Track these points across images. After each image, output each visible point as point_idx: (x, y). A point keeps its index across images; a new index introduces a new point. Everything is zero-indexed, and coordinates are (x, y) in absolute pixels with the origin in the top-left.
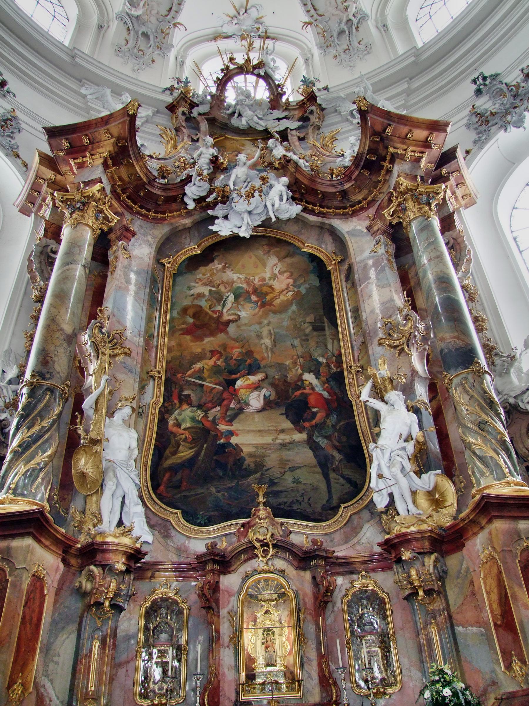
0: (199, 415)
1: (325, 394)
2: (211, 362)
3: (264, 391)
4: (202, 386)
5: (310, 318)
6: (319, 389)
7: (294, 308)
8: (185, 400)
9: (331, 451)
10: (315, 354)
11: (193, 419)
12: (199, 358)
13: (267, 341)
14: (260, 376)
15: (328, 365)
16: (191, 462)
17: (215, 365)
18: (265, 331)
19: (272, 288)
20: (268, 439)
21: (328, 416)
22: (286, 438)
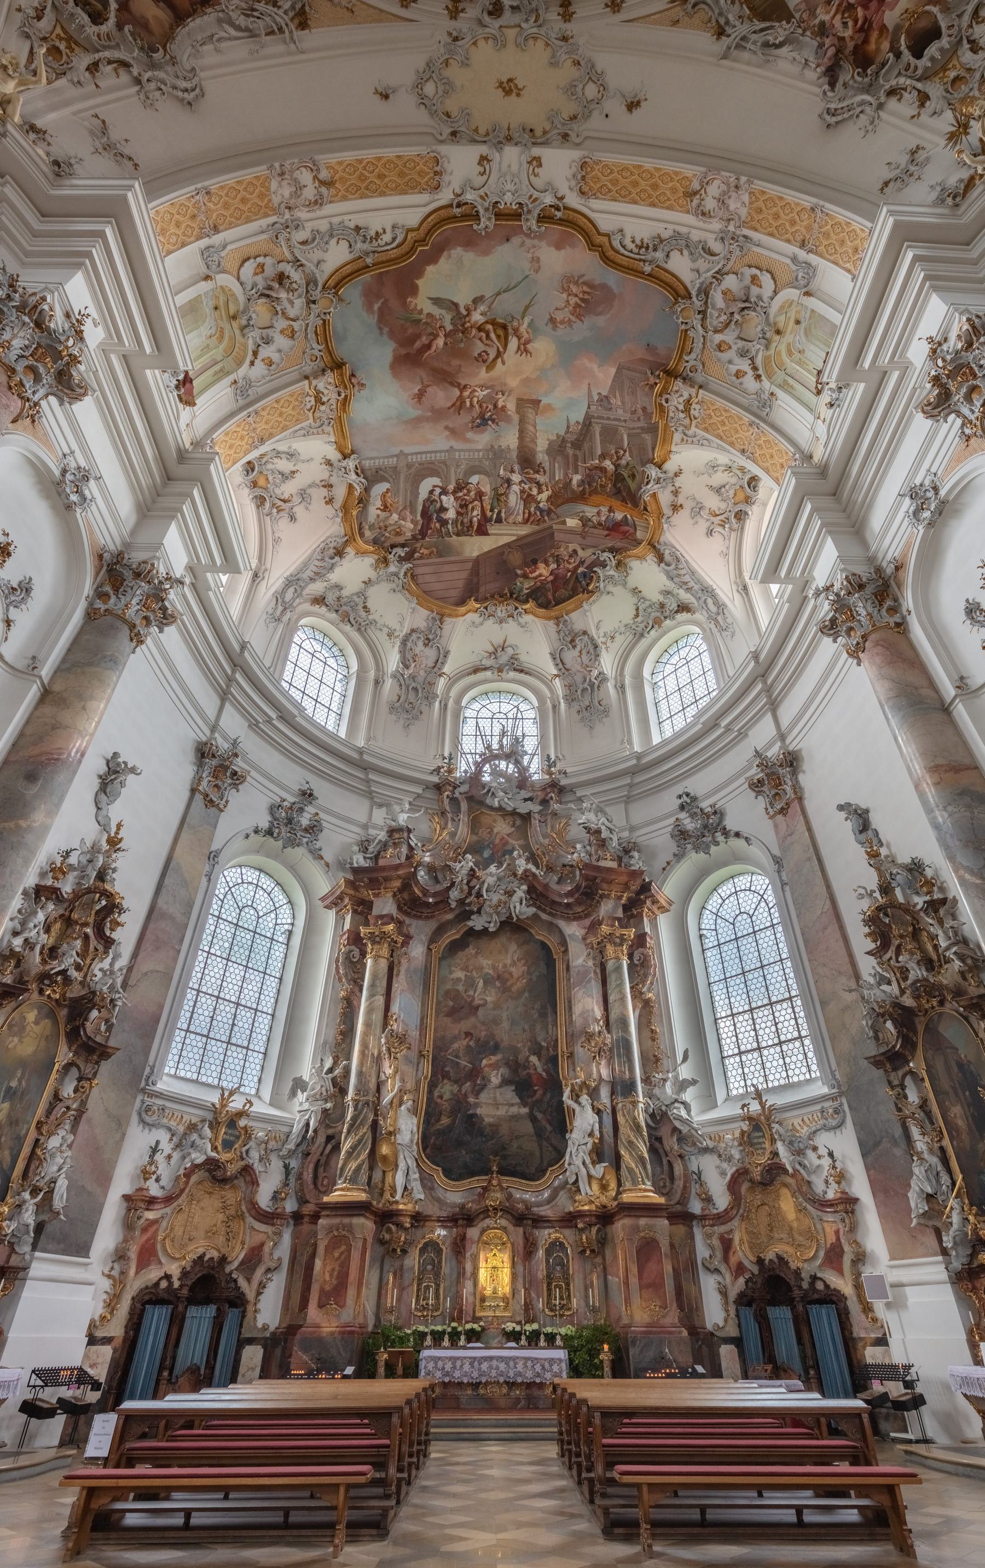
0: (455, 1088)
1: (544, 1074)
2: (465, 1042)
3: (501, 1070)
4: (458, 1063)
5: (537, 1006)
6: (540, 1070)
7: (526, 994)
8: (446, 1076)
9: (544, 1123)
10: (539, 1039)
11: (452, 1092)
12: (456, 1038)
13: (505, 1025)
14: (499, 1056)
15: (548, 1049)
16: (450, 1128)
17: (468, 1046)
18: (504, 1015)
19: (511, 974)
20: (502, 1112)
21: (544, 1094)
22: (514, 1110)
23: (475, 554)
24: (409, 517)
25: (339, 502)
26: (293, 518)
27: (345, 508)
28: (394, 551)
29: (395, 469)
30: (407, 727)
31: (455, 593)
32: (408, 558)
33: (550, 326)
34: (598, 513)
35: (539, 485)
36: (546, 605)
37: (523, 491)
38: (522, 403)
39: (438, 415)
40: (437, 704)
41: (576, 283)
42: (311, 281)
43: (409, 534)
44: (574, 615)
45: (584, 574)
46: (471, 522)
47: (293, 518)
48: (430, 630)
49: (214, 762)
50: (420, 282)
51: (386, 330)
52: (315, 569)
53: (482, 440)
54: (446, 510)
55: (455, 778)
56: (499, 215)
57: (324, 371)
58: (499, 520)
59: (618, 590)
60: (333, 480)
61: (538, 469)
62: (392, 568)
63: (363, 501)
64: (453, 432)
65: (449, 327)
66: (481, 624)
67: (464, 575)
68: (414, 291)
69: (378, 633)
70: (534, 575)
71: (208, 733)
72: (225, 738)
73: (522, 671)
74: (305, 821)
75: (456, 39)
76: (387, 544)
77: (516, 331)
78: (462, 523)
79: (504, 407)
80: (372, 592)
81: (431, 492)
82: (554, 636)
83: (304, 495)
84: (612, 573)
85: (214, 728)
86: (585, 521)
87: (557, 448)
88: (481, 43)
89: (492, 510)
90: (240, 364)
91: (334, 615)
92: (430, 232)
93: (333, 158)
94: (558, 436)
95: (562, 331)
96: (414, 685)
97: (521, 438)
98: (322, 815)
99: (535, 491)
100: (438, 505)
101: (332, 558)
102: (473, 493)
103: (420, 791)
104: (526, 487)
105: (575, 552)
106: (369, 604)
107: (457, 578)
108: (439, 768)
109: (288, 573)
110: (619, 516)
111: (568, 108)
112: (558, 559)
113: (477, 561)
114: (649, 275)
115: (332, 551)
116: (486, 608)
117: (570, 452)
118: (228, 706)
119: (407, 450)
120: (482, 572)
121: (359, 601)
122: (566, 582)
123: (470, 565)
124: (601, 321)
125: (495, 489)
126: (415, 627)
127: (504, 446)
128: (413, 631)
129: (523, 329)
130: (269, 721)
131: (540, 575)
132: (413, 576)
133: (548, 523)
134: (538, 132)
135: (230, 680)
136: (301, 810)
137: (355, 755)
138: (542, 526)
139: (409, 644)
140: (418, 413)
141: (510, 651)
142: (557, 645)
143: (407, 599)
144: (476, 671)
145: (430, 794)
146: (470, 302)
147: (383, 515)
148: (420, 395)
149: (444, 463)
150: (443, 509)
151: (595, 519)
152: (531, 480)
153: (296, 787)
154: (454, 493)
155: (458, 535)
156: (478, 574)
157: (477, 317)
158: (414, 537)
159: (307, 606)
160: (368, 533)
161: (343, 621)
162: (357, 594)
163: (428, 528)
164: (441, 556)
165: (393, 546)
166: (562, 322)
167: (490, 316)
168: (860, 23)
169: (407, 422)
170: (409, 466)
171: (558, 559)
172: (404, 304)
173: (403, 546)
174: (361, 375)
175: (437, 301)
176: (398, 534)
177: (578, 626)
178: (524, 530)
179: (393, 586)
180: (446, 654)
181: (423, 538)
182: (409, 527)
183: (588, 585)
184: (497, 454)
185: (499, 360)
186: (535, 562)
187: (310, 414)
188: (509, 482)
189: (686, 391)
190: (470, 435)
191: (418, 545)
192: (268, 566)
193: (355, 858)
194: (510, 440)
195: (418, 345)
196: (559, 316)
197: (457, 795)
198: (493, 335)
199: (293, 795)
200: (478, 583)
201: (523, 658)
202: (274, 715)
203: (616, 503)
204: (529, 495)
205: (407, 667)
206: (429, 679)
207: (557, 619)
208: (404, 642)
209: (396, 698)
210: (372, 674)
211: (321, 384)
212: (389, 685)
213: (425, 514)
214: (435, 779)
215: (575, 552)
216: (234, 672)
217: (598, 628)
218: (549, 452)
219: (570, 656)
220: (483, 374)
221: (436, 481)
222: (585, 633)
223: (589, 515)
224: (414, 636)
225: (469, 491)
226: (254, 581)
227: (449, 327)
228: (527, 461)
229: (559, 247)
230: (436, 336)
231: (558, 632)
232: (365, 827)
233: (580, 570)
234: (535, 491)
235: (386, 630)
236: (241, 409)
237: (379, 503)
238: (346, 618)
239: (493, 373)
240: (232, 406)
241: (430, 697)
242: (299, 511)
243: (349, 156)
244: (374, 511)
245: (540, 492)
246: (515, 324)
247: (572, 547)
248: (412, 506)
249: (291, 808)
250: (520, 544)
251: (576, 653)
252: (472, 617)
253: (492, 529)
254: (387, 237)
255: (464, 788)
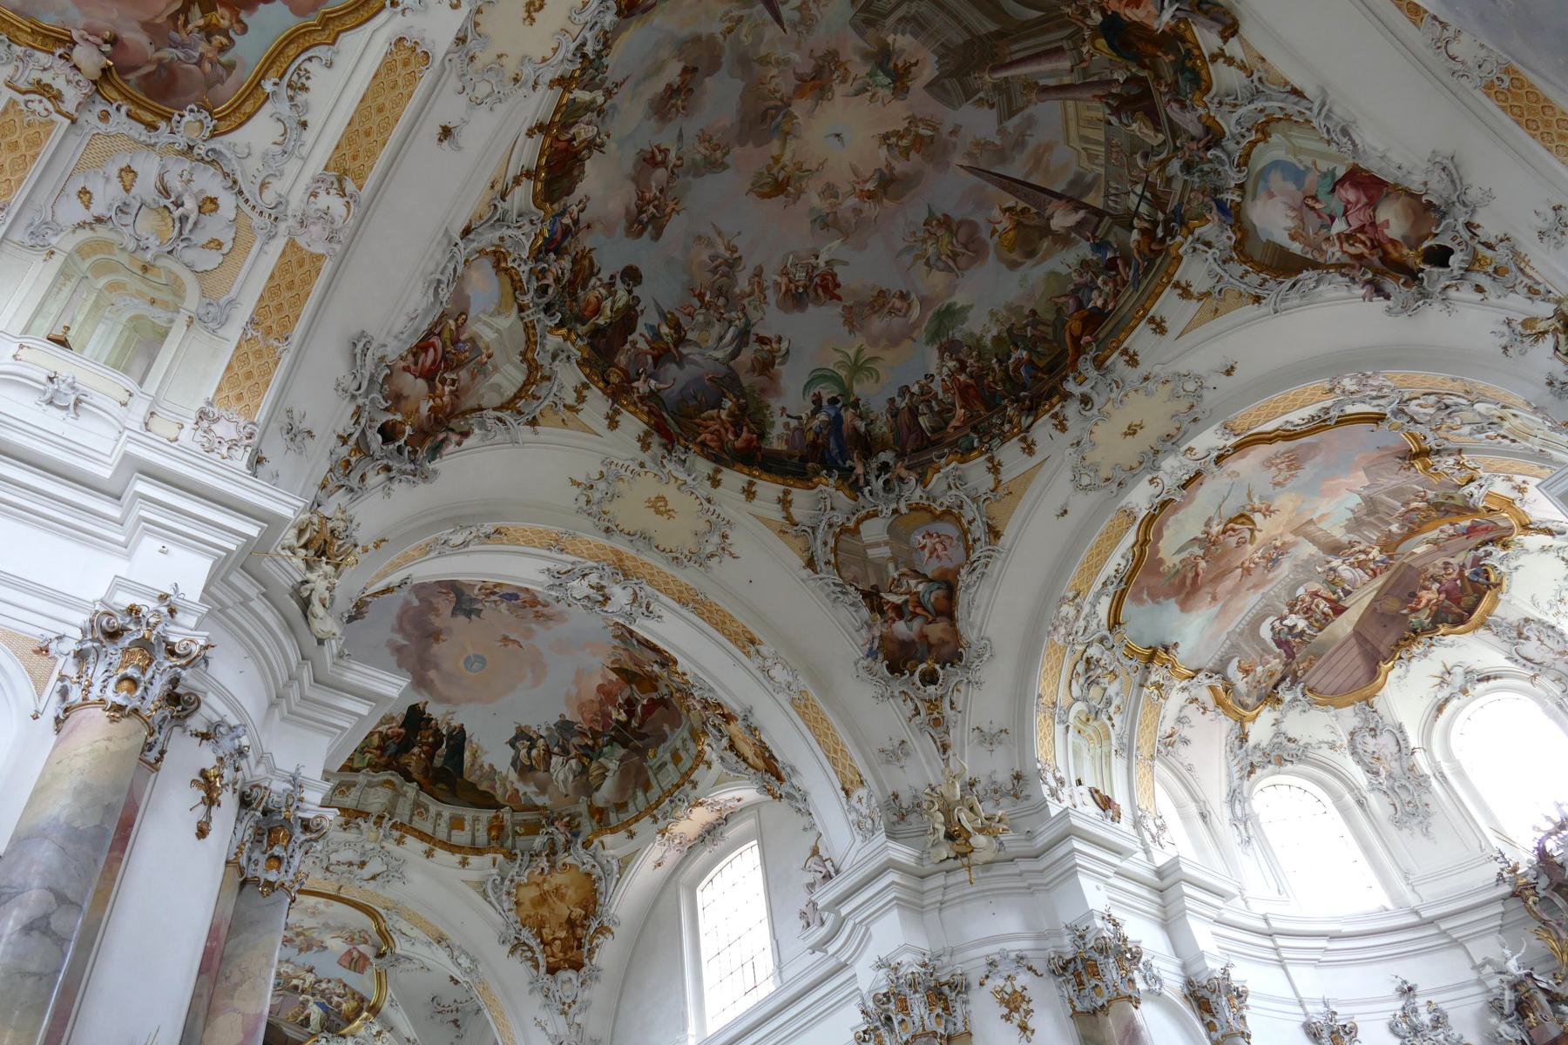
23: (1350, 629)
24: (1269, 658)
25: (1211, 704)
26: (1186, 742)
27: (1219, 703)
28: (1279, 688)
29: (1232, 646)
30: (1426, 833)
31: (1361, 672)
32: (1295, 681)
33: (1278, 489)
34: (1441, 531)
35: (1364, 552)
36: (1460, 620)
37: (1351, 564)
38: (1295, 532)
39: (1235, 591)
40: (1435, 784)
41: (1277, 457)
42: (1102, 640)
43: (1280, 667)
44: (1499, 611)
45: (1476, 574)
46: (1324, 613)
47: (1186, 742)
48: (1366, 720)
49: (1325, 1034)
50: (1160, 555)
51: (1161, 599)
52: (1237, 768)
53: (1285, 568)
54: (1295, 625)
55: (1525, 875)
56: (1184, 486)
57: (1147, 668)
58: (1348, 593)
59: (1524, 559)
60: (1194, 693)
61: (1351, 545)
62: (1288, 697)
63: (1229, 688)
64: (1256, 586)
65: (1201, 553)
66: (1408, 671)
67: (1356, 651)
68: (1161, 562)
69: (1320, 752)
70: (1423, 604)
71: (1300, 1010)
72: (1314, 1003)
73: (1488, 678)
74: (1425, 1018)
75: (1078, 443)
76: (1270, 689)
77: (1254, 510)
78: (1317, 621)
79: (1284, 544)
80: (1284, 727)
81: (1273, 629)
82: (1495, 640)
83: (1180, 720)
84: (1504, 553)
85: (1301, 1003)
86: (1435, 542)
87: (1356, 524)
88: (1095, 429)
89: (1334, 593)
90: (1108, 737)
91: (1270, 767)
92: (1146, 533)
93: (1070, 583)
94: (1349, 520)
95: (1289, 484)
96: (1397, 784)
97: (1313, 541)
98: (1434, 999)
99: (1362, 557)
100: (1286, 629)
101: (1241, 747)
102: (1308, 599)
103: (1501, 909)
104: (1352, 560)
105: (1447, 564)
106: (1291, 735)
107: (1353, 659)
108: (1500, 874)
109: (1224, 795)
110: (1467, 523)
111: (1183, 405)
112: (1434, 579)
113: (1357, 634)
114: (1337, 423)
115: (1237, 743)
116: (1400, 658)
117: (1371, 519)
118: (1290, 969)
119: (1230, 629)
120: (1368, 637)
121: (1282, 739)
122: (1463, 589)
123: (1353, 641)
124: (1319, 459)
125: (1325, 581)
126: (1351, 729)
127: (1305, 557)
128: (1352, 734)
129: (1257, 503)
130: (1326, 950)
131: (1429, 601)
132: (1311, 690)
133: (1397, 563)
134: (1173, 432)
135: (1276, 949)
136: (1415, 1011)
137: (1413, 919)
138: (1393, 569)
139: (1361, 752)
140: (1219, 605)
141: (1459, 671)
142: (1507, 647)
143: (1322, 710)
144: (1440, 709)
145: (1515, 904)
146: (1203, 528)
147: (1250, 678)
148: (1214, 598)
149: (1266, 605)
150: (1291, 628)
151: (1442, 535)
152: (1352, 555)
153: (1390, 989)
154: (1291, 612)
155: (1321, 630)
156: (1367, 641)
157: (1216, 529)
158: (1286, 665)
159: (1246, 784)
160: (1250, 701)
161: (1281, 765)
162: (1277, 735)
163: (1291, 648)
164: (1321, 656)
165: (1275, 687)
166: (1286, 479)
167: (1224, 521)
168: (1368, 243)
169: (1217, 617)
170: (1241, 634)
171: (1434, 579)
172: (1160, 574)
173: (1283, 679)
174: (1170, 640)
175: (1180, 550)
176: (1271, 676)
177: (1514, 617)
178: (1380, 581)
179: (1300, 708)
180: (1401, 729)
181: (1294, 658)
182: (1276, 664)
183: (1488, 579)
184: (1306, 566)
185: (1256, 533)
186: (1413, 595)
187: (1161, 700)
188: (1333, 569)
189: (1451, 461)
190: (1271, 575)
191: (1294, 666)
192: (1202, 797)
193: (1500, 1030)
194: (1307, 549)
195: (1188, 582)
196: (1280, 479)
197: (1542, 894)
198: (1237, 527)
199: (1396, 1000)
200: (1374, 648)
201: (1477, 666)
202: (1323, 943)
203: (1454, 519)
204: (1359, 562)
205: (1377, 773)
206: (1406, 766)
207: (1483, 624)
208: (1354, 753)
209: (1392, 808)
210: (1349, 799)
211: (1153, 678)
212: (1373, 800)
213: (1279, 644)
214: (1506, 889)
215: (1447, 564)
216: (1273, 941)
217: (1535, 604)
218: (1349, 530)
219: (1530, 648)
220: (1250, 548)
221: (1271, 619)
222: (1527, 620)
223: (1435, 536)
224: (1358, 739)
225: (1303, 601)
226: (1206, 823)
227: (1201, 553)
228: (1336, 549)
229: (1242, 457)
230: (1197, 565)
231: (1497, 634)
232: (1480, 982)
233: (1467, 573)
234: (1362, 557)
235: (1325, 746)
236: (1129, 759)
237: (1240, 675)
238: (1281, 761)
239: (1257, 542)
240: (1125, 762)
241: (1421, 782)
242: (1186, 732)
243: (1075, 570)
244: (1241, 683)
245: (1367, 553)
246: (1248, 507)
247: (1439, 562)
248: (1267, 650)
249: (1405, 1015)
250: (1383, 593)
251: (1534, 642)
252: (1391, 675)
253: (1347, 602)
254: (1123, 563)
255: (1544, 881)
